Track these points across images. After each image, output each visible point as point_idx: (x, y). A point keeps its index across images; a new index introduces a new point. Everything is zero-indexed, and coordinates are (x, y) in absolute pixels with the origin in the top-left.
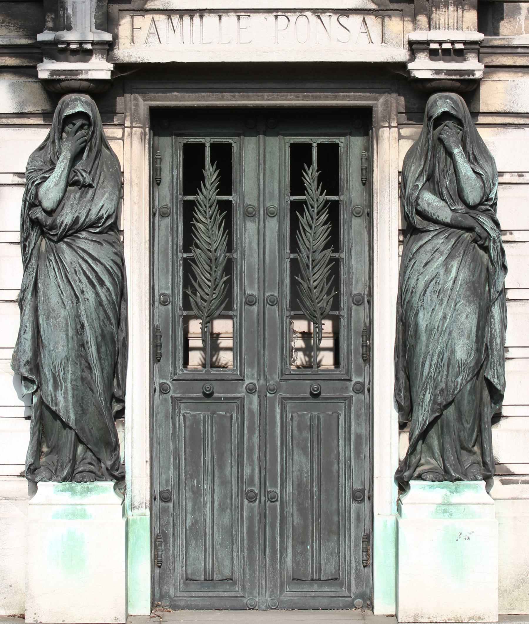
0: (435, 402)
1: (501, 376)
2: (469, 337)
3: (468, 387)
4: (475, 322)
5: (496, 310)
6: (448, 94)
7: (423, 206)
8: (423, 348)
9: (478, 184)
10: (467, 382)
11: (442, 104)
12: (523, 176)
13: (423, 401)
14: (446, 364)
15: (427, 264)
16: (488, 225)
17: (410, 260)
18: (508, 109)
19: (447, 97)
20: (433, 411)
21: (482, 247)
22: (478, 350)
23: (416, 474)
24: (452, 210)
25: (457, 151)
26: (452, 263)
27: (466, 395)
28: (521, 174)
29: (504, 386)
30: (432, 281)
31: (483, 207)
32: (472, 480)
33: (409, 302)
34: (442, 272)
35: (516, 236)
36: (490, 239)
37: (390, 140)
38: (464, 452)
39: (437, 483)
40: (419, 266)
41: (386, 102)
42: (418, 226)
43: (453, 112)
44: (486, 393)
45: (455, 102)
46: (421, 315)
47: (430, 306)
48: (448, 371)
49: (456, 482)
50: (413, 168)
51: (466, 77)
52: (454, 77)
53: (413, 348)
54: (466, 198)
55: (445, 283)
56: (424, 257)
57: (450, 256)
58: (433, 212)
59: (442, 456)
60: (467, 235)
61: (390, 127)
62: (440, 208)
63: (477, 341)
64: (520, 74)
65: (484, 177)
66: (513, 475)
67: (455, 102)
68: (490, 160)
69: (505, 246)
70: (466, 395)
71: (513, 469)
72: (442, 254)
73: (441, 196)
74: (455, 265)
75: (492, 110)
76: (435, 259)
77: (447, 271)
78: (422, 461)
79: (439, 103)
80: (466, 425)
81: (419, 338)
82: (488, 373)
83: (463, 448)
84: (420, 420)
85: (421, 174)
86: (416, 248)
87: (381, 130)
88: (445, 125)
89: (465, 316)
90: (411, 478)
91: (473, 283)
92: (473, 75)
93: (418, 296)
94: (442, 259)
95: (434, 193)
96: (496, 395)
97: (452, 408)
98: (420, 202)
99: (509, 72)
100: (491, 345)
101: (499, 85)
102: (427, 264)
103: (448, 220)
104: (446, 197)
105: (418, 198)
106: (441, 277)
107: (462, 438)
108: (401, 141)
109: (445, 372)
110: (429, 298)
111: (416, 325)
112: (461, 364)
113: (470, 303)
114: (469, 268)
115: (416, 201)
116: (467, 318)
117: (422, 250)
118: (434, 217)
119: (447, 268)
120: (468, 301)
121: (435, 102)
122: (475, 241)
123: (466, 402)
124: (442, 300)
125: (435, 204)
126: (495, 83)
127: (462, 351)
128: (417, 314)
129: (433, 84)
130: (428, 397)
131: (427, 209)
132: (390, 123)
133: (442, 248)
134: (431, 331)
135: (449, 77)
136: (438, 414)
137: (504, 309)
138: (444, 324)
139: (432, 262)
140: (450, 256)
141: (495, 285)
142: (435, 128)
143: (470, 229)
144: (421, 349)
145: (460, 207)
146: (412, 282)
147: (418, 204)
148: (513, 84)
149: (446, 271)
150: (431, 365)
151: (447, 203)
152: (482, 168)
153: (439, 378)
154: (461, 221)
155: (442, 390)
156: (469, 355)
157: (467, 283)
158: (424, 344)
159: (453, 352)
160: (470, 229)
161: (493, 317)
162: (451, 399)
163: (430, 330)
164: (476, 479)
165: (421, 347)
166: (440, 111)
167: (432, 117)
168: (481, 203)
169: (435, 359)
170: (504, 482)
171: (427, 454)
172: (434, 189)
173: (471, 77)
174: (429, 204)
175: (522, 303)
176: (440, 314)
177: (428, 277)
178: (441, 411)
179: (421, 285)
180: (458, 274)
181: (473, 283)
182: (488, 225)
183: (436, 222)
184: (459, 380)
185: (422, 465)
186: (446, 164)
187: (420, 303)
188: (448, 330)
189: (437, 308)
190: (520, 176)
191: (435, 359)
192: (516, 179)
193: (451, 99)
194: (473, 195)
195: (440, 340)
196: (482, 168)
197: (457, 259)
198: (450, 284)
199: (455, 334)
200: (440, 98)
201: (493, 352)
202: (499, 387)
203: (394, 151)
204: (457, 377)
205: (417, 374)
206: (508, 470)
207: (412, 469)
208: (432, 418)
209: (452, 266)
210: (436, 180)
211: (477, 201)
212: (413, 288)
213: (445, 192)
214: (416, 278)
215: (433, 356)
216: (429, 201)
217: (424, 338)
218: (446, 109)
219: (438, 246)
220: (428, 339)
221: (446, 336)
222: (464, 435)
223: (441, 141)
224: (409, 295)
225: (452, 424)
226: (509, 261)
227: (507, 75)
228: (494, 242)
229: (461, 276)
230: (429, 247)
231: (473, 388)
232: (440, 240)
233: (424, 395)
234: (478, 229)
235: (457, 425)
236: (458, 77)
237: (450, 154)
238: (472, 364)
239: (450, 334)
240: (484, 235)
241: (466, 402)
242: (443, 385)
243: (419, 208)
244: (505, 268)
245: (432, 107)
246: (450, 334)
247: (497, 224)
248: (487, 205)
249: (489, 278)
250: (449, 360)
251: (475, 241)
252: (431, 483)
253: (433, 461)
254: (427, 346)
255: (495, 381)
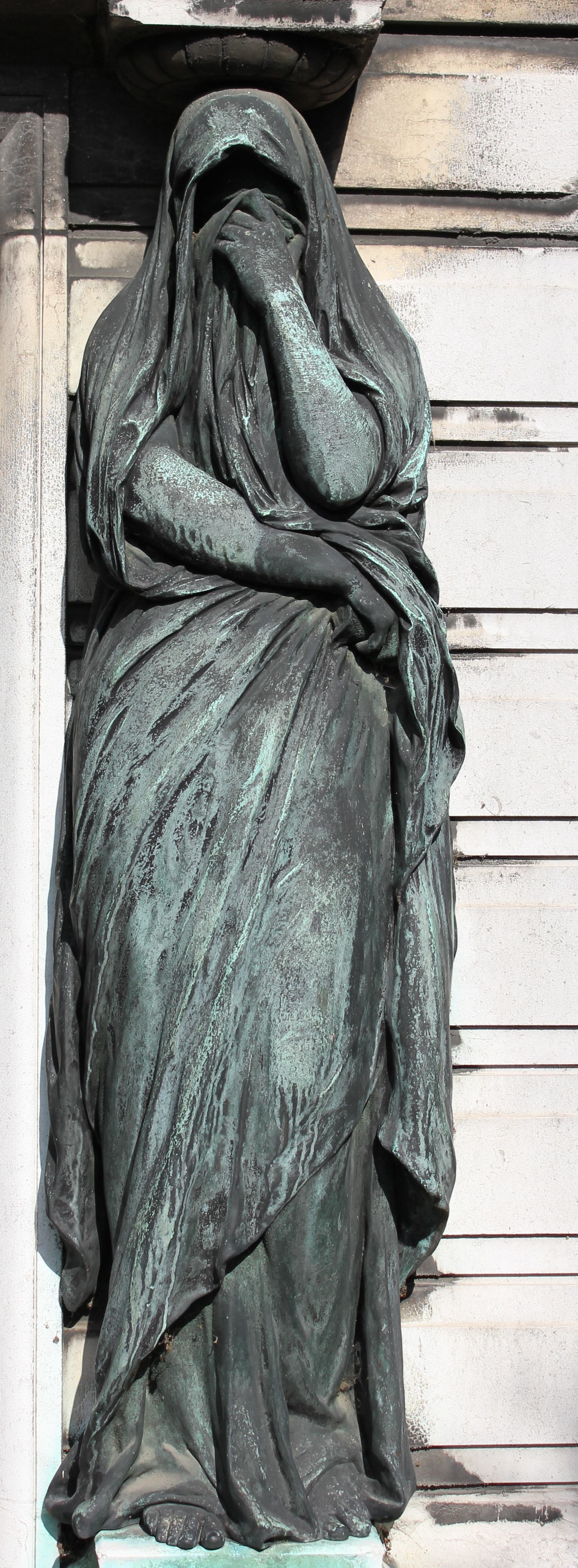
0: (192, 1246)
1: (441, 1148)
2: (322, 1001)
3: (320, 1189)
4: (345, 943)
5: (421, 899)
6: (249, 92)
7: (154, 502)
8: (151, 1040)
9: (363, 423)
10: (315, 1172)
11: (227, 123)
12: (513, 417)
13: (146, 1245)
14: (235, 1102)
15: (164, 722)
16: (399, 580)
17: (103, 709)
18: (464, 177)
19: (246, 103)
20: (187, 1280)
21: (368, 661)
22: (356, 1049)
23: (122, 1507)
24: (260, 519)
25: (282, 299)
26: (263, 717)
27: (311, 1218)
28: (505, 410)
29: (450, 1179)
30: (182, 786)
31: (379, 515)
32: (333, 1537)
33: (97, 865)
34: (221, 755)
35: (491, 631)
36: (403, 633)
37: (39, 281)
38: (299, 1423)
39: (199, 1552)
40: (134, 731)
41: (26, 146)
42: (132, 581)
43: (266, 151)
44: (381, 1204)
45: (274, 119)
46: (141, 915)
47: (178, 882)
48: (241, 1130)
49: (274, 1550)
50: (117, 367)
51: (320, 24)
52: (272, 23)
53: (114, 1035)
54: (314, 474)
55: (235, 794)
56: (154, 697)
57: (255, 695)
58: (189, 525)
59: (220, 1440)
60: (318, 619)
61: (40, 233)
62: (216, 513)
63: (353, 1017)
64: (507, 57)
65: (382, 400)
66: (475, 1485)
67: (274, 119)
68: (403, 347)
69: (457, 664)
70: (311, 1218)
71: (477, 1464)
72: (222, 686)
73: (221, 470)
74: (271, 727)
75: (407, 179)
76: (196, 706)
77: (243, 750)
78: (147, 1456)
79: (217, 120)
80: (307, 1325)
81: (135, 1003)
82: (391, 1135)
83: (297, 1407)
84: (137, 1314)
85: (146, 388)
86: (127, 661)
87: (10, 243)
88: (241, 206)
89: (307, 921)
90: (104, 1521)
91: (341, 795)
92: (347, 15)
93: (131, 842)
94: (223, 703)
95: (199, 463)
96: (420, 1213)
97: (254, 1267)
98: (140, 488)
99: (467, 47)
100: (405, 1028)
101: (434, 92)
102: (164, 722)
103: (247, 558)
104: (240, 469)
105: (133, 473)
106: (219, 772)
107: (294, 1372)
108: (79, 287)
109: (232, 1135)
110: (173, 852)
111: (125, 953)
112: (294, 1104)
113: (327, 872)
114: (324, 740)
115: (128, 484)
116: (319, 930)
117: (149, 668)
118: (195, 546)
119: (241, 738)
120: (320, 865)
121: (203, 119)
122: (346, 638)
123: (309, 1242)
124: (222, 859)
125: (197, 495)
126: (417, 84)
127: (301, 1055)
128: (127, 911)
129: (197, 50)
130: (165, 1228)
131: (166, 513)
132: (40, 220)
133: (224, 663)
134: (179, 975)
135: (255, 23)
136: (202, 1290)
137: (447, 893)
138: (227, 950)
139: (185, 715)
140: (255, 695)
141: (419, 804)
142: (198, 225)
143: (329, 595)
144: (141, 1044)
145: (292, 509)
146: (111, 792)
147: (132, 498)
148: (483, 88)
149: (235, 748)
150: (177, 1109)
151: (242, 492)
152: (375, 370)
153: (210, 1155)
154: (293, 563)
155: (219, 1201)
156: (322, 1068)
157: (318, 795)
158: (153, 1023)
159: (265, 1059)
160: (329, 595)
161: (410, 922)
162: (253, 1235)
163: (176, 974)
164: (347, 1532)
165: (142, 1035)
166: (220, 145)
167: (189, 173)
168: (369, 499)
169: (193, 1086)
170: (443, 1516)
171: (164, 1430)
172: (196, 446)
173: (338, 23)
174: (174, 497)
175: (511, 868)
176: (216, 915)
177: (169, 772)
178: (216, 1279)
179: (143, 802)
180: (283, 759)
181: (341, 795)
182: (399, 580)
183: (201, 564)
184: (285, 1163)
185: (147, 1469)
186: (241, 353)
187: (138, 871)
188: (243, 975)
189: (201, 891)
190: (503, 417)
191: (193, 1086)
192: (489, 428)
193: (263, 109)
194: (343, 468)
195: (214, 1014)
196: (375, 370)
197: (281, 705)
198: (251, 798)
199: (271, 990)
200: (221, 104)
201: (410, 1055)
202: (433, 1186)
203: (54, 321)
204: (278, 1152)
205: (125, 1134)
206: (457, 1469)
207: (105, 1492)
208: (182, 1306)
209: (262, 730)
210: (202, 412)
211: (359, 488)
212: (114, 813)
213: (236, 454)
214: (122, 775)
215: (184, 1073)
216: (175, 485)
217: (152, 1000)
218: (244, 139)
219: (209, 655)
220: (169, 1006)
221: (236, 998)
222: (301, 1361)
223: (224, 269)
224: (98, 837)
225: (254, 1325)
226: (471, 720)
227: (461, 58)
228: (421, 642)
229: (298, 767)
230: (173, 659)
231: (337, 1190)
232: (216, 633)
233: (151, 1221)
234: (360, 593)
235: (276, 1329)
236: (288, 23)
237: (254, 315)
238: (335, 1104)
239: (251, 987)
240: (382, 614)
241: (309, 1242)
242: (222, 1183)
243: (137, 512)
244: (455, 741)
245: (189, 139)
246: (251, 987)
247: (427, 579)
248: (390, 506)
249: (399, 781)
250: (247, 1086)
251: (346, 638)
252: (175, 1553)
253: (185, 1459)
254: (165, 1032)
255: (419, 1164)
